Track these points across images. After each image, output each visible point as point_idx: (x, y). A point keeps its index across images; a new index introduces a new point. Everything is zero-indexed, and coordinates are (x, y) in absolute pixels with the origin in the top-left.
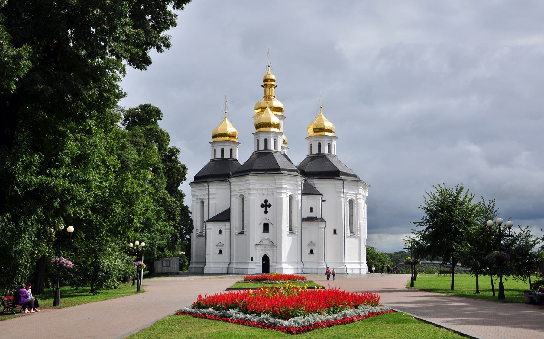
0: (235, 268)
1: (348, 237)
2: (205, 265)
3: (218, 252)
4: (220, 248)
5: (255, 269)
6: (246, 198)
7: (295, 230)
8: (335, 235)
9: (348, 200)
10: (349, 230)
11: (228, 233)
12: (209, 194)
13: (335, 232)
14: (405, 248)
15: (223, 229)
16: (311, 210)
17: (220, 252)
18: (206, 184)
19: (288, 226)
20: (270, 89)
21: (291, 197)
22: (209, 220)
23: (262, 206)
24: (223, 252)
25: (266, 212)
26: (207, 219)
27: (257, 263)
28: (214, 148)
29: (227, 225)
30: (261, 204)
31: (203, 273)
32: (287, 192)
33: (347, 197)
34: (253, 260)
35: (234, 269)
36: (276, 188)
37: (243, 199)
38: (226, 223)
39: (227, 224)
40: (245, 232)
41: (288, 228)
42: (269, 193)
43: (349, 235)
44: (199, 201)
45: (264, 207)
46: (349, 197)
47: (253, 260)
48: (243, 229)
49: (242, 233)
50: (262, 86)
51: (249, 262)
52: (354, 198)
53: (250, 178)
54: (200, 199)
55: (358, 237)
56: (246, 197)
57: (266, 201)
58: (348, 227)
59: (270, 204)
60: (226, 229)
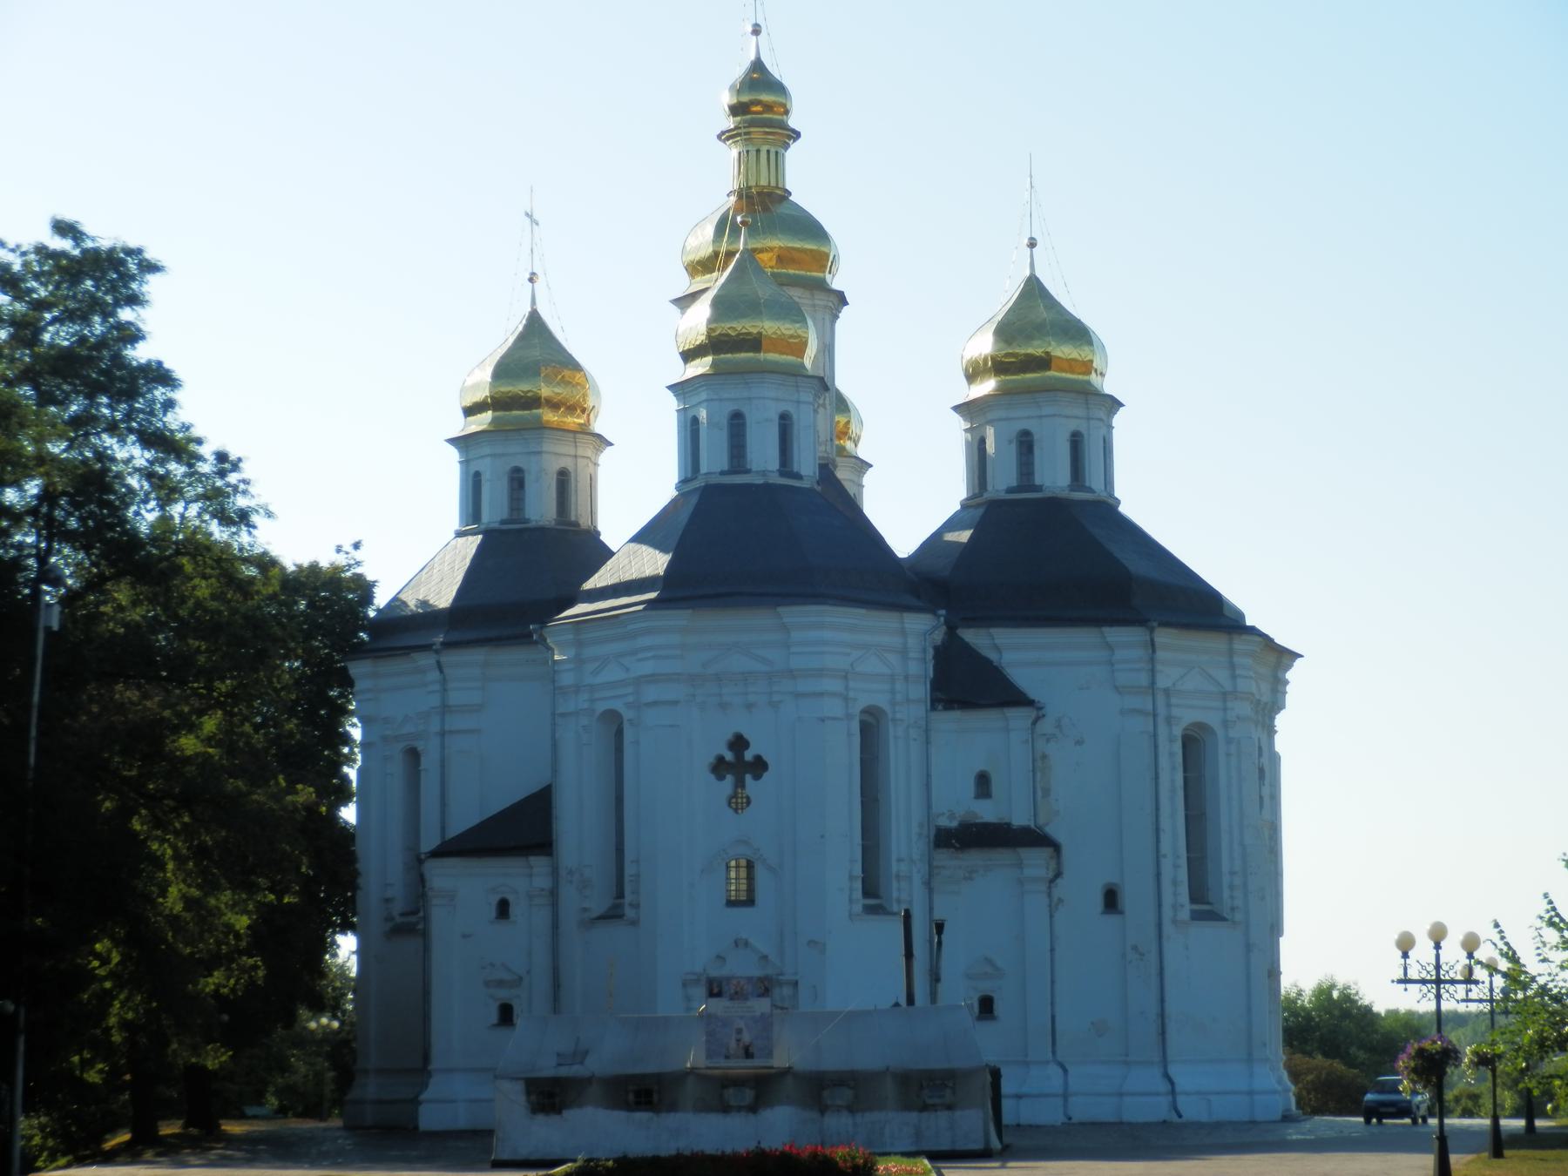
2: (425, 1086)
3: (494, 1016)
4: (504, 994)
7: (895, 895)
8: (1113, 919)
9: (1178, 732)
10: (1184, 890)
13: (1111, 900)
14: (1400, 981)
16: (983, 784)
17: (506, 1015)
18: (425, 660)
19: (858, 870)
20: (763, 155)
21: (870, 719)
23: (720, 767)
25: (738, 802)
28: (473, 468)
30: (711, 759)
31: (416, 1128)
32: (851, 694)
33: (1175, 712)
36: (791, 674)
37: (619, 733)
38: (532, 859)
39: (539, 863)
41: (858, 885)
43: (1185, 914)
45: (729, 779)
46: (1187, 716)
48: (620, 894)
49: (614, 914)
50: (719, 137)
52: (1213, 719)
57: (739, 743)
58: (1183, 875)
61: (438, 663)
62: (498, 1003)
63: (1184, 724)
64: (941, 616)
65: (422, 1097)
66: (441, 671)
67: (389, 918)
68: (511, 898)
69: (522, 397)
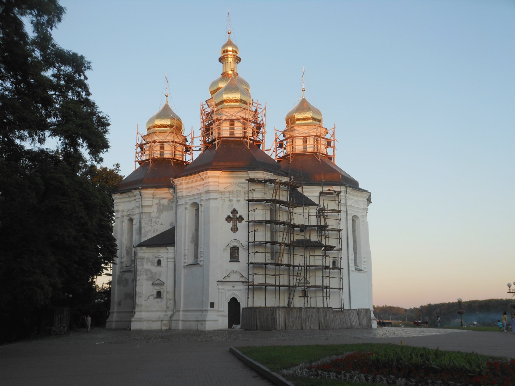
0: (183, 321)
1: (353, 271)
5: (217, 321)
6: (203, 207)
11: (171, 265)
12: (141, 206)
15: (163, 258)
17: (159, 294)
18: (136, 192)
22: (141, 245)
23: (228, 219)
24: (164, 294)
26: (137, 243)
27: (221, 311)
29: (169, 251)
34: (214, 307)
35: (180, 323)
37: (197, 210)
39: (171, 249)
40: (201, 261)
42: (239, 198)
44: (126, 220)
47: (214, 307)
48: (196, 257)
51: (207, 310)
53: (209, 175)
54: (127, 215)
55: (366, 272)
56: (201, 206)
57: (234, 212)
59: (240, 216)
60: (167, 258)
61: (140, 192)
62: (157, 291)
63: (353, 215)
64: (292, 178)
65: (132, 320)
66: (141, 195)
67: (122, 268)
68: (161, 259)
69: (164, 124)
